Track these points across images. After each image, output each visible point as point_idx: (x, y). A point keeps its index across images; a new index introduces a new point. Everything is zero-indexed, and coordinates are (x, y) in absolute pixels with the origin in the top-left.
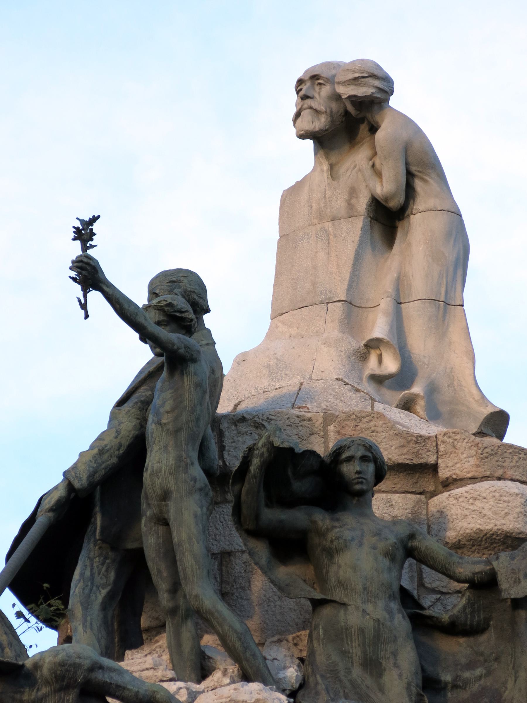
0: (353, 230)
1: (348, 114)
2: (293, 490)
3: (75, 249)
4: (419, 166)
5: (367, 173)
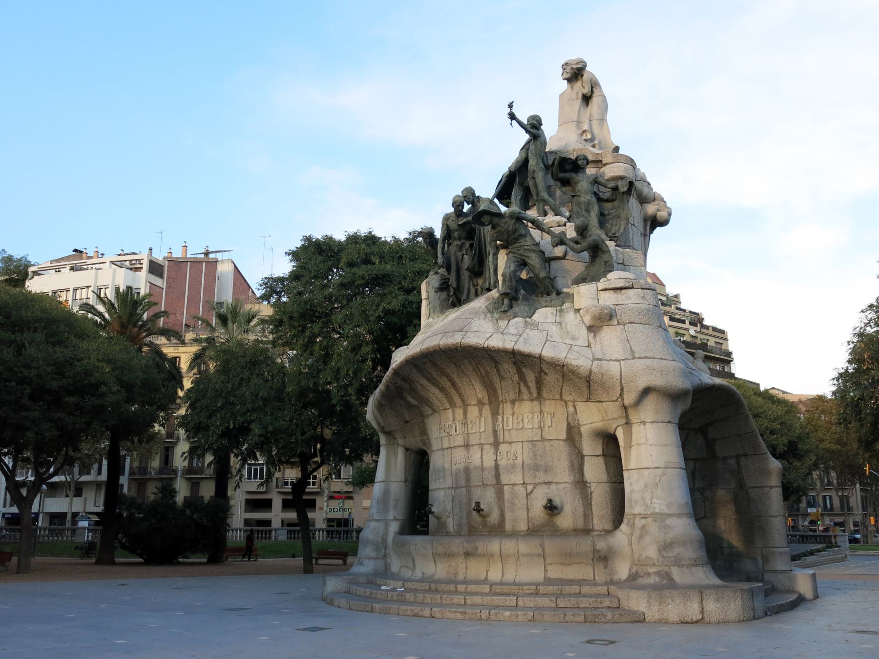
0: (579, 102)
1: (575, 73)
2: (566, 168)
3: (509, 110)
4: (594, 85)
5: (581, 88)
